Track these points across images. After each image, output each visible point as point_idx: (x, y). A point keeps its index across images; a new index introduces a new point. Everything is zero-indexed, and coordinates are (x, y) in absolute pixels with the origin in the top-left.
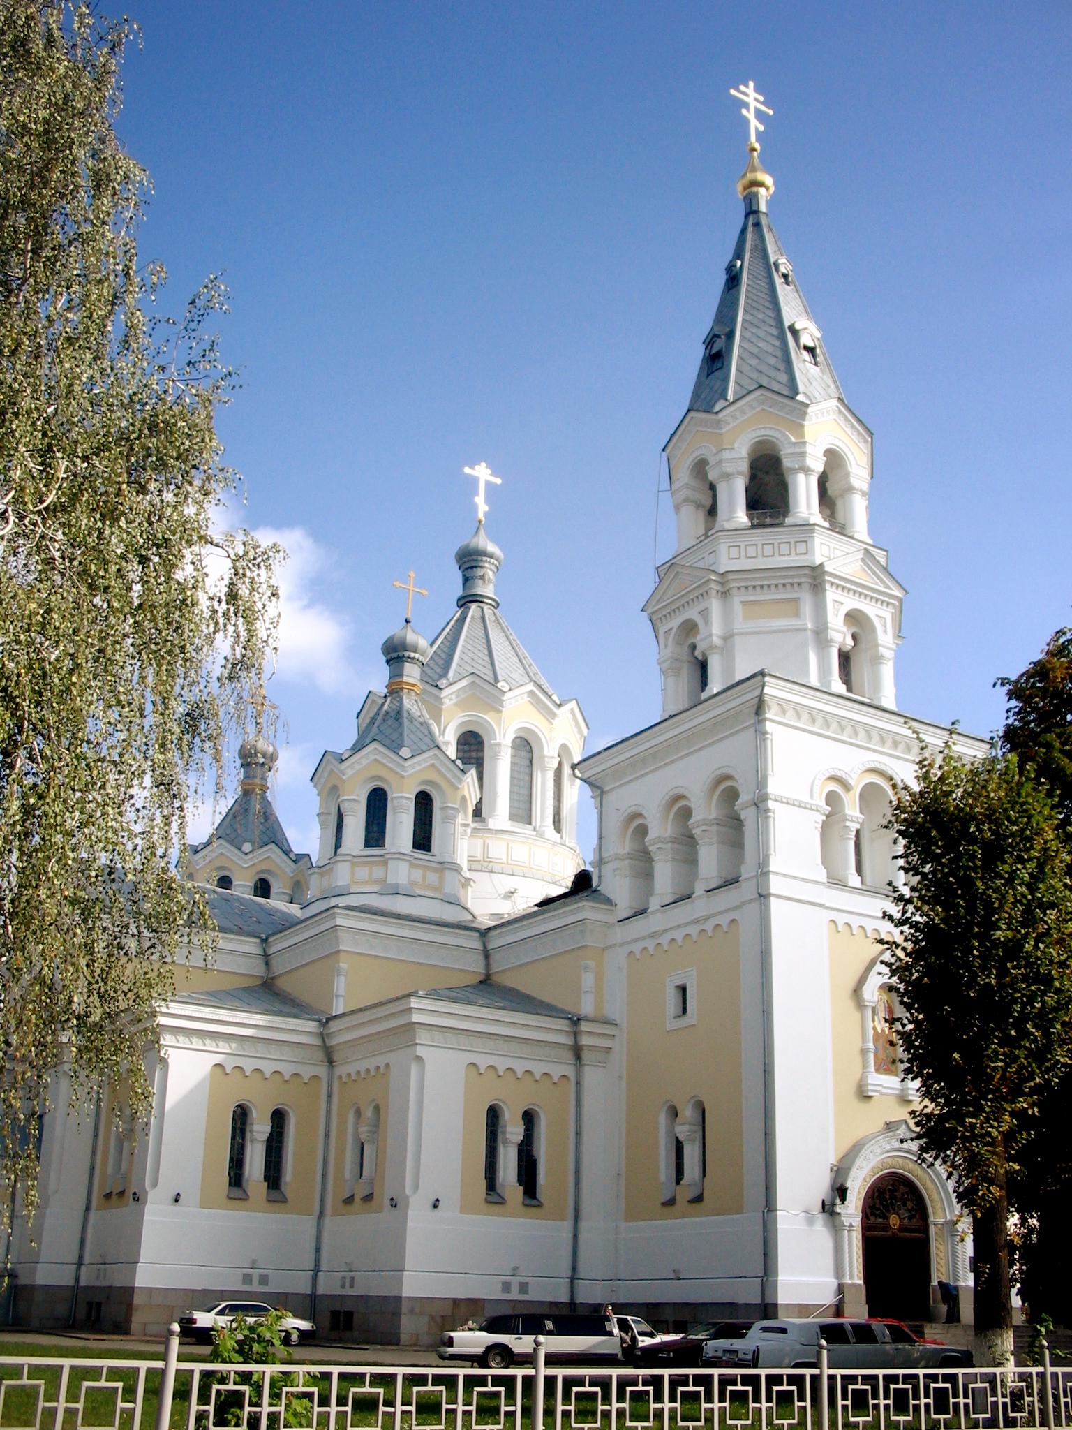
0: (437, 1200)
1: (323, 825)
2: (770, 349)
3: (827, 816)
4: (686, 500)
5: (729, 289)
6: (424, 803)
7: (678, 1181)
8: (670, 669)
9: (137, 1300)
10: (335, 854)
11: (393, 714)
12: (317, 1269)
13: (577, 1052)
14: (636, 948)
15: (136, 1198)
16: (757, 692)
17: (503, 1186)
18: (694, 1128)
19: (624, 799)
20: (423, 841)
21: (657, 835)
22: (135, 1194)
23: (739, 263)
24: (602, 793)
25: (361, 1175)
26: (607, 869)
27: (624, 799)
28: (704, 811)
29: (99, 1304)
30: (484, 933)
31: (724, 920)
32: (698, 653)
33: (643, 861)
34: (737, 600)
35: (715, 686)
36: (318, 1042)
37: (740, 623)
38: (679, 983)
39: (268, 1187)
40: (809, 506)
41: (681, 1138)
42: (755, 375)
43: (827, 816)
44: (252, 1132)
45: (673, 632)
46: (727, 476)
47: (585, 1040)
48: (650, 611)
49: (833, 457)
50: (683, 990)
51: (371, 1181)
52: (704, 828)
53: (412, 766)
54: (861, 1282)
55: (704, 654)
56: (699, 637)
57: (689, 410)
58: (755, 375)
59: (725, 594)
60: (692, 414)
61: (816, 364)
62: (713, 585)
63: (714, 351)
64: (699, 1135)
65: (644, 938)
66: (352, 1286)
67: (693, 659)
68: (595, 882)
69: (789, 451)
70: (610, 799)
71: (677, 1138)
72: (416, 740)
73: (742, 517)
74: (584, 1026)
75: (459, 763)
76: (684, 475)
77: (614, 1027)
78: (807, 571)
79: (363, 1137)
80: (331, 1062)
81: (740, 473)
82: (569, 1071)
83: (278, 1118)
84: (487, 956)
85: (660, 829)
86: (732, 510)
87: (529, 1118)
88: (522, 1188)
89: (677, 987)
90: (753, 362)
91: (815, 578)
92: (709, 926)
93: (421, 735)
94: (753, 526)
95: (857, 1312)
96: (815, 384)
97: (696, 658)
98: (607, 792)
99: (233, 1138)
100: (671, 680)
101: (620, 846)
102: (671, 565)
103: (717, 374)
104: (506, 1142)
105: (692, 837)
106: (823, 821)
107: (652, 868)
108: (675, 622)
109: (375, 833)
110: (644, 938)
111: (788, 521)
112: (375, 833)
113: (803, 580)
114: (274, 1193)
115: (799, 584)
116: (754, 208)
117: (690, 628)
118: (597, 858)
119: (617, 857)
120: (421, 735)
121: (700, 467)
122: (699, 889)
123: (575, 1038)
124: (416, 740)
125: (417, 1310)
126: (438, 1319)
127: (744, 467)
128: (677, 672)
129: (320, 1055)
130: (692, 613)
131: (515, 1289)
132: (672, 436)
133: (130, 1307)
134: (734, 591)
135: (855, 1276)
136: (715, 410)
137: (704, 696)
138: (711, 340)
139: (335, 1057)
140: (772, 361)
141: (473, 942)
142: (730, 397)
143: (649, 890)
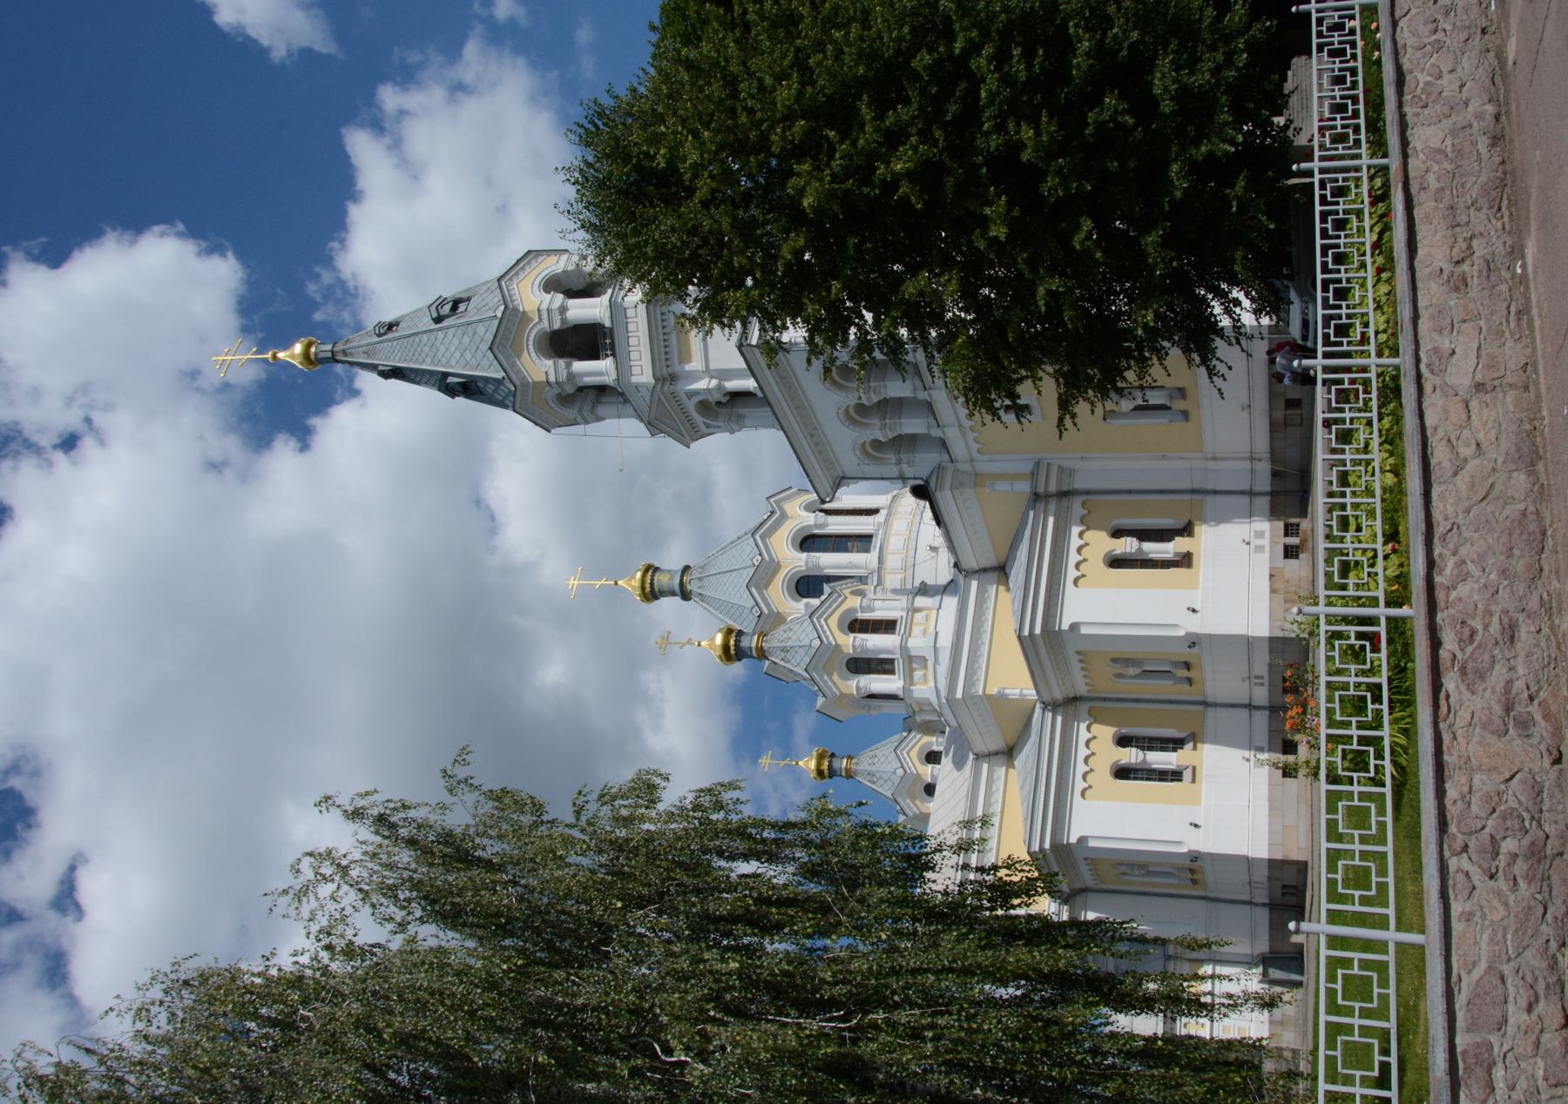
9: (1279, 856)
14: (974, 446)
16: (756, 350)
19: (848, 459)
24: (844, 478)
26: (909, 472)
27: (848, 459)
29: (1284, 887)
32: (724, 400)
33: (906, 443)
37: (695, 365)
55: (725, 395)
65: (965, 440)
68: (920, 482)
105: (879, 403)
107: (907, 435)
110: (965, 440)
113: (658, 311)
115: (662, 314)
122: (922, 395)
133: (1284, 863)
137: (760, 394)
139: (1071, 695)
143: (926, 438)
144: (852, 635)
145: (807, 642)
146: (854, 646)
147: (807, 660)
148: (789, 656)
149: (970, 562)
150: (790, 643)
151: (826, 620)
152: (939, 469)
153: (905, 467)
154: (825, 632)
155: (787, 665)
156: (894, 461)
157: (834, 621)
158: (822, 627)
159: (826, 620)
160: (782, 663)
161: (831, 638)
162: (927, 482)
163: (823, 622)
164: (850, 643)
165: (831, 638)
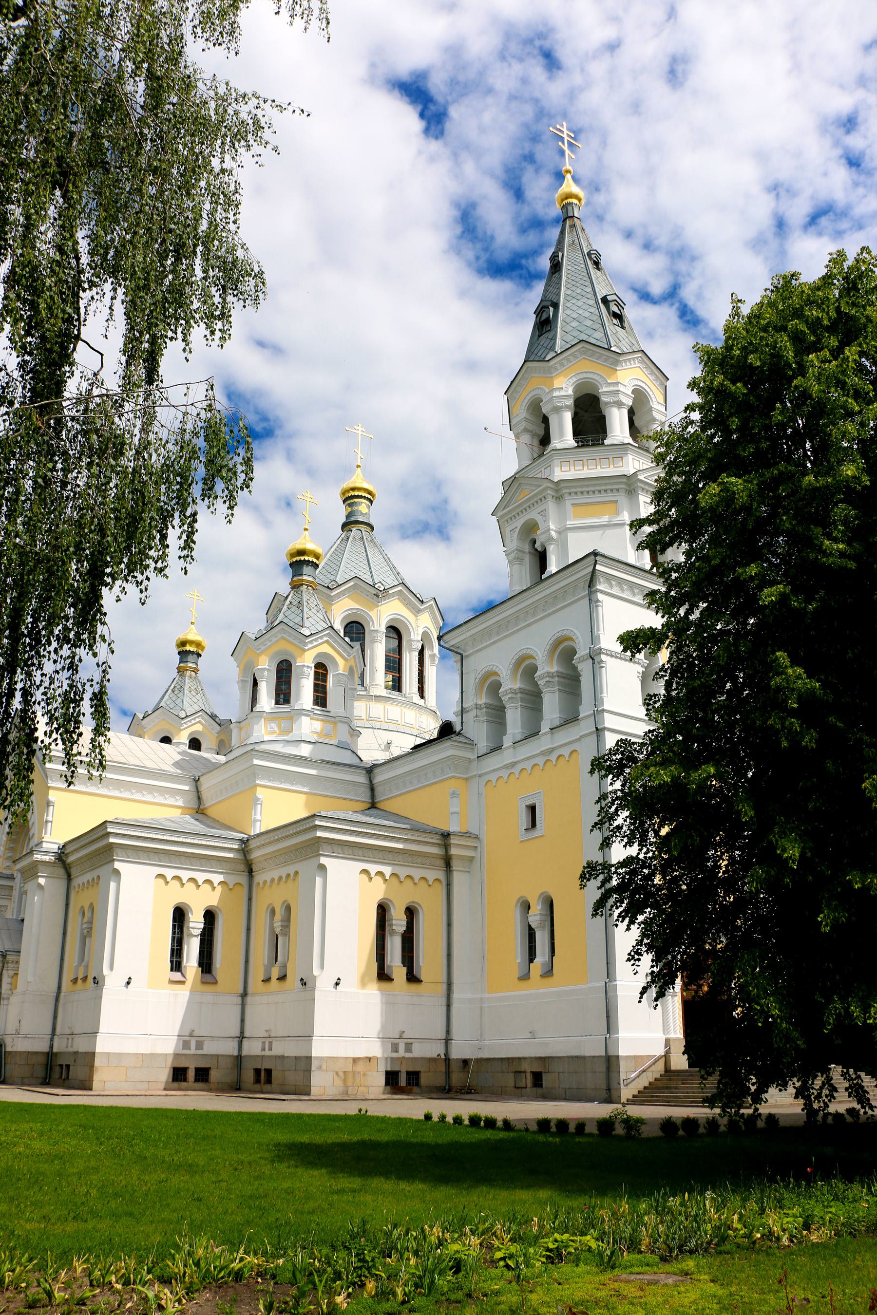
0: (339, 979)
1: (242, 689)
2: (587, 314)
3: (646, 668)
4: (526, 430)
5: (553, 273)
6: (321, 671)
7: (531, 960)
8: (514, 559)
10: (252, 711)
11: (295, 603)
12: (241, 1037)
13: (448, 862)
15: (95, 981)
17: (390, 967)
18: (543, 917)
20: (321, 699)
21: (509, 687)
22: (95, 978)
23: (560, 254)
25: (276, 961)
28: (547, 667)
30: (370, 770)
31: (566, 752)
34: (568, 503)
35: (553, 567)
36: (239, 856)
38: (530, 802)
39: (202, 972)
40: (622, 431)
41: (533, 926)
42: (576, 333)
43: (646, 668)
44: (188, 927)
45: (517, 530)
46: (558, 410)
47: (454, 851)
48: (500, 513)
49: (639, 395)
50: (532, 809)
51: (285, 966)
52: (547, 679)
53: (311, 642)
54: (682, 1037)
56: (539, 532)
57: (525, 362)
58: (576, 333)
59: (559, 498)
60: (528, 364)
61: (623, 327)
62: (549, 492)
63: (543, 319)
64: (548, 924)
66: (270, 1049)
67: (533, 551)
69: (605, 389)
70: (469, 663)
71: (530, 926)
72: (314, 622)
73: (569, 440)
74: (453, 841)
75: (347, 639)
76: (522, 412)
77: (475, 840)
78: (624, 480)
79: (277, 931)
80: (251, 871)
81: (567, 407)
82: (441, 875)
83: (210, 916)
84: (372, 789)
85: (510, 684)
86: (562, 434)
87: (410, 912)
88: (405, 969)
89: (527, 806)
90: (575, 324)
91: (629, 485)
92: (553, 757)
93: (318, 620)
94: (578, 447)
95: (680, 1062)
96: (623, 342)
97: (536, 550)
98: (467, 656)
99: (174, 933)
100: (516, 567)
101: (478, 699)
102: (514, 478)
103: (545, 335)
104: (393, 933)
106: (643, 672)
108: (519, 523)
109: (283, 695)
111: (606, 442)
112: (283, 695)
114: (208, 977)
116: (570, 214)
117: (530, 528)
118: (460, 708)
119: (477, 707)
120: (318, 620)
121: (535, 406)
123: (446, 849)
124: (314, 622)
125: (324, 1067)
126: (341, 1074)
127: (570, 402)
128: (520, 560)
129: (242, 867)
130: (533, 515)
131: (402, 1048)
132: (512, 382)
134: (567, 497)
135: (677, 1032)
136: (547, 359)
137: (544, 576)
138: (540, 310)
139: (254, 868)
140: (589, 323)
141: (362, 779)
142: (558, 349)
144: (313, 665)
145: (307, 623)
146: (303, 666)
147: (291, 624)
148: (294, 609)
149: (379, 777)
150: (306, 609)
151: (327, 642)
152: (471, 744)
153: (474, 713)
154: (316, 640)
155: (285, 607)
156: (480, 702)
157: (326, 649)
158: (321, 638)
159: (327, 642)
160: (287, 602)
161: (310, 646)
162: (459, 734)
163: (325, 639)
164: (305, 663)
165: (310, 646)
